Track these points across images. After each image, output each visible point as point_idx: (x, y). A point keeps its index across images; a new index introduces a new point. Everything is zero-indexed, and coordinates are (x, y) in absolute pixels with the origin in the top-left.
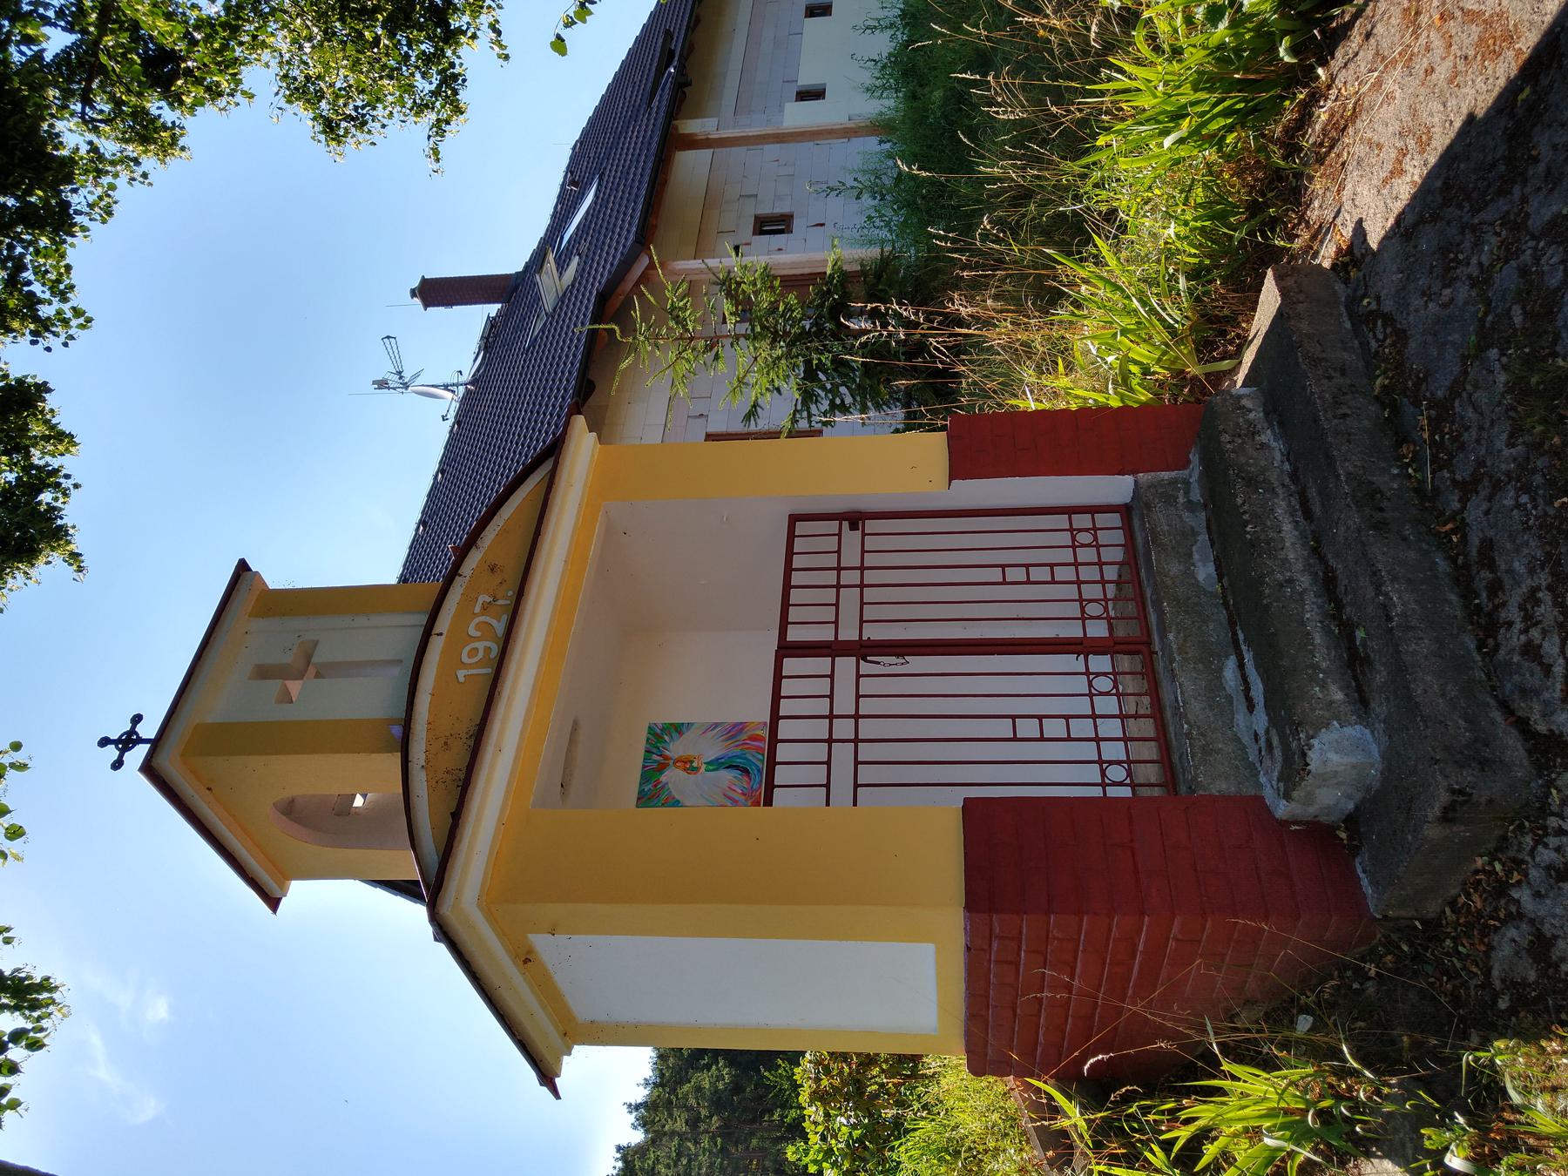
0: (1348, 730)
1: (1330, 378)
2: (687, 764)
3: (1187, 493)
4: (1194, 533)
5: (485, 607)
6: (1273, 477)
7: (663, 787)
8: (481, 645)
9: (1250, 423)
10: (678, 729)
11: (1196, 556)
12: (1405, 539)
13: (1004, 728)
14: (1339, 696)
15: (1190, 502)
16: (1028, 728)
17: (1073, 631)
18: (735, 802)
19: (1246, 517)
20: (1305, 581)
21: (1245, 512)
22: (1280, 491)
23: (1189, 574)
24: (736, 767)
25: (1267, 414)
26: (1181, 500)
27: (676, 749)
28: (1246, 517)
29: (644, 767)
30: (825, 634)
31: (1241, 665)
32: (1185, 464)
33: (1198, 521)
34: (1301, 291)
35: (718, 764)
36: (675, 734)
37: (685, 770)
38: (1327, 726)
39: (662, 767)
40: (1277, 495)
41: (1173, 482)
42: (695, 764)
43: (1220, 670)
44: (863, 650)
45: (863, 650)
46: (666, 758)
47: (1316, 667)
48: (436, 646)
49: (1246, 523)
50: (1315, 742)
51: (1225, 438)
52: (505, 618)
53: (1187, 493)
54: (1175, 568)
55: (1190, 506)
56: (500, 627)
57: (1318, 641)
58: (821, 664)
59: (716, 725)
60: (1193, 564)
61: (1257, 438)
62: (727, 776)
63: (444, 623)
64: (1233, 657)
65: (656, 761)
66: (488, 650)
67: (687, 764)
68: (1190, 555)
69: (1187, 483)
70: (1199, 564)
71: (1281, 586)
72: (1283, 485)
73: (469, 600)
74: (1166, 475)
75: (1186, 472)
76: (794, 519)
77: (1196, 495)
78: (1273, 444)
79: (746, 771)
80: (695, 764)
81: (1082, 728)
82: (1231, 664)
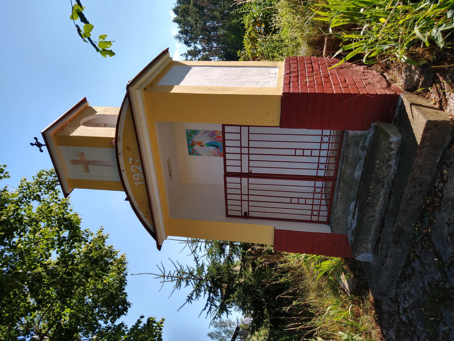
0: (368, 255)
1: (414, 187)
2: (200, 144)
3: (364, 142)
4: (360, 159)
5: (133, 163)
6: (386, 181)
7: (195, 151)
8: (137, 175)
9: (390, 156)
10: (195, 132)
11: (357, 168)
12: (401, 246)
13: (288, 200)
14: (370, 246)
15: (363, 146)
17: (313, 173)
18: (216, 156)
19: (370, 194)
20: (377, 216)
21: (370, 193)
22: (385, 186)
23: (353, 174)
24: (215, 146)
25: (398, 152)
26: (361, 144)
27: (196, 139)
28: (370, 194)
29: (188, 144)
30: (238, 170)
31: (356, 205)
32: (367, 128)
33: (363, 154)
34: (430, 140)
35: (209, 144)
36: (194, 135)
37: (200, 146)
38: (363, 253)
39: (193, 145)
40: (384, 187)
41: (361, 136)
42: (202, 144)
43: (350, 205)
44: (250, 175)
45: (250, 175)
46: (194, 142)
47: (368, 240)
48: (124, 174)
49: (369, 196)
50: (358, 256)
51: (378, 162)
52: (140, 166)
53: (364, 142)
54: (348, 171)
55: (363, 148)
56: (140, 169)
57: (372, 233)
58: (237, 180)
59: (206, 132)
60: (355, 171)
61: (389, 162)
62: (213, 148)
63: (123, 167)
64: (355, 202)
65: (191, 143)
66: (139, 176)
67: (200, 144)
68: (355, 167)
69: (366, 137)
70: (357, 171)
71: (370, 217)
72: (388, 184)
73: (126, 161)
74: (359, 132)
75: (367, 132)
76: (227, 216)
77: (367, 144)
78: (393, 166)
79: (217, 147)
80: (202, 144)
81: (316, 153)
82: (354, 203)
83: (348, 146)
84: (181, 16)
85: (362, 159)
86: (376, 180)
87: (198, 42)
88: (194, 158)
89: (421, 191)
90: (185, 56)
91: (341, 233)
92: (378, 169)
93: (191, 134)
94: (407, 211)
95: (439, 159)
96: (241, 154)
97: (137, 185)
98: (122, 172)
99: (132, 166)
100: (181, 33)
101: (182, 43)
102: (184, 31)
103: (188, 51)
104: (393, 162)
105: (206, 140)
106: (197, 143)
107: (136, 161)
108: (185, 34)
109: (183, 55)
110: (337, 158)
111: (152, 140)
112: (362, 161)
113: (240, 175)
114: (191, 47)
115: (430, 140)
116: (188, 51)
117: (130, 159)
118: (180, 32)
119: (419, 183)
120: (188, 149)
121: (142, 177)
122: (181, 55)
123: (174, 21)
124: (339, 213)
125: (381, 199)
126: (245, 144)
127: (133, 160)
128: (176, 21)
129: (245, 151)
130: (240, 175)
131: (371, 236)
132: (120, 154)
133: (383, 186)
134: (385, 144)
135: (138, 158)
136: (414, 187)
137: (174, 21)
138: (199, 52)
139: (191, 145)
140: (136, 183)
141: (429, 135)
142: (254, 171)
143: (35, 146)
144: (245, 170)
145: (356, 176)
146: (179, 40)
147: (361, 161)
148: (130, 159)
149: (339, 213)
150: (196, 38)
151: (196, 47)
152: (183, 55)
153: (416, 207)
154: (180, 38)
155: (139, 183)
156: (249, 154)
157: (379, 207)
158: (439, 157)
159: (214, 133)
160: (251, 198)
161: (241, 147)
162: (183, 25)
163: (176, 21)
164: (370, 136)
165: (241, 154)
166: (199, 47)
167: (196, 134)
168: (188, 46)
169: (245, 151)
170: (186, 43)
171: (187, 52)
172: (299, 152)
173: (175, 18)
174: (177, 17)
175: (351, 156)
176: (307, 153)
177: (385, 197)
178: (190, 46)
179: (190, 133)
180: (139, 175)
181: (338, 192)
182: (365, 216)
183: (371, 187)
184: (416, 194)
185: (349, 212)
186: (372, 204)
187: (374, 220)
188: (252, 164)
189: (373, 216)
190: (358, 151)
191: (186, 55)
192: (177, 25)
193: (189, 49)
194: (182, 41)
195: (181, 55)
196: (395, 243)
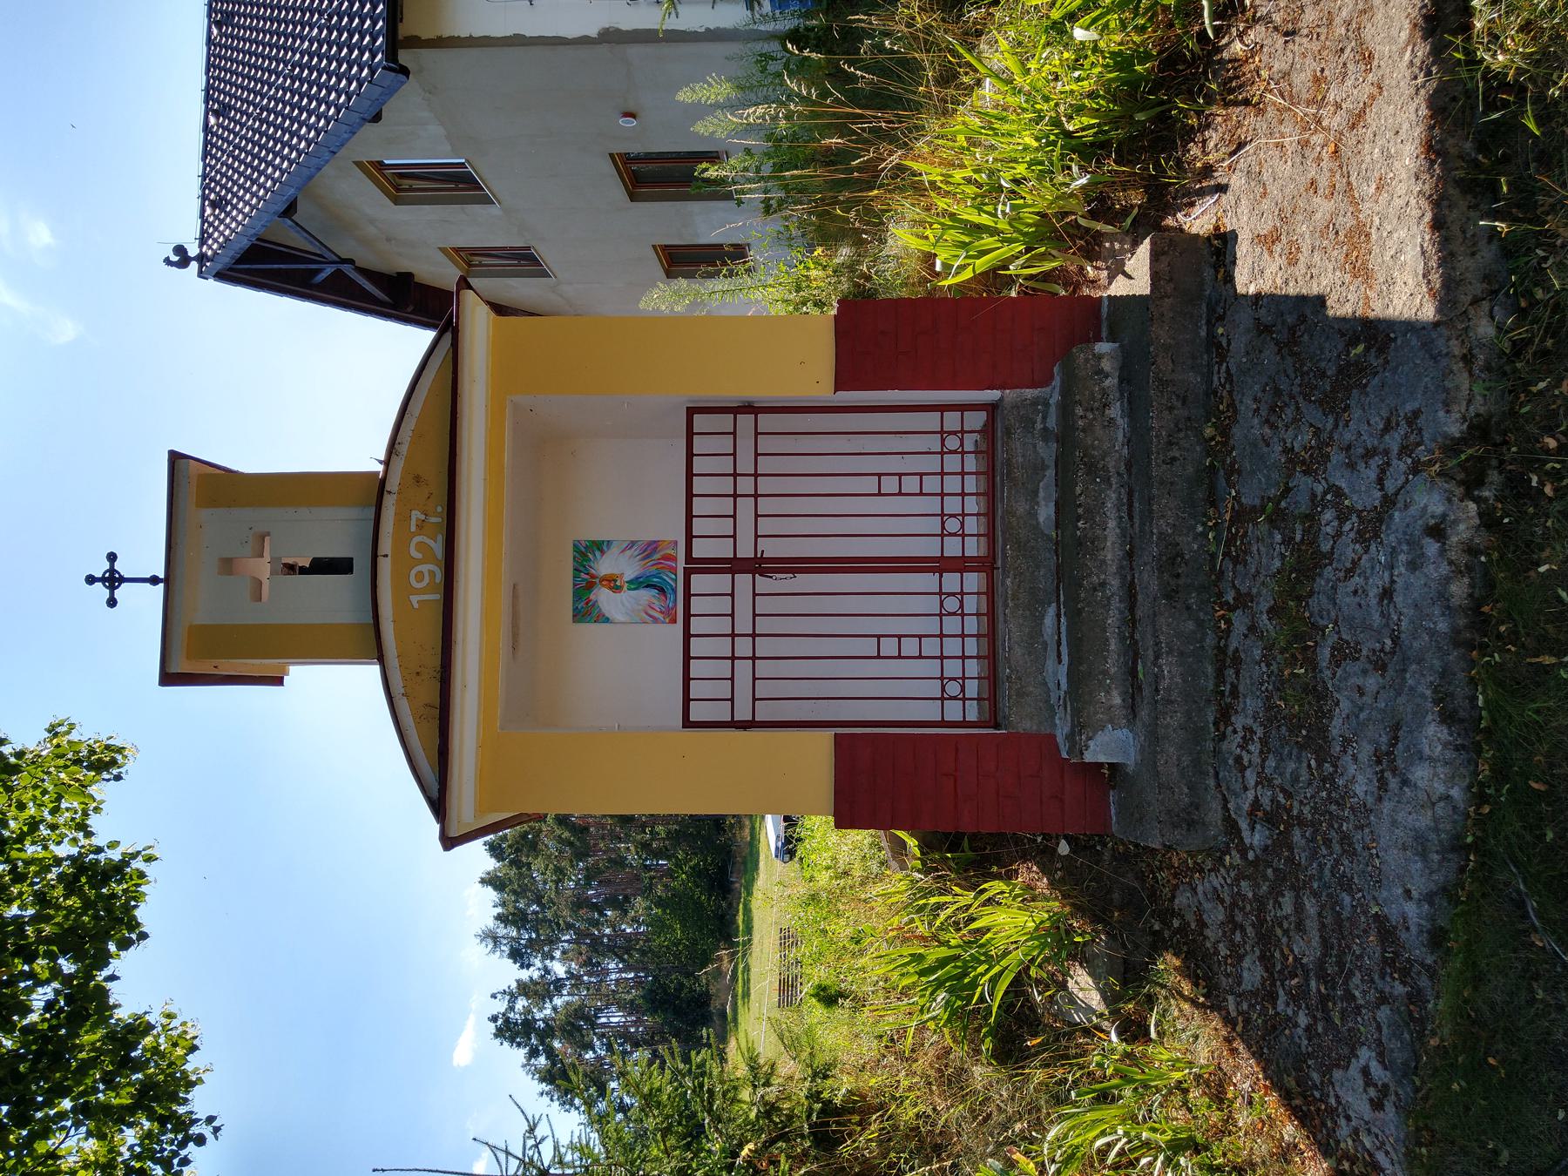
0: (1118, 733)
1: (1171, 409)
2: (612, 583)
3: (1044, 418)
4: (1044, 467)
5: (421, 526)
6: (1111, 463)
7: (593, 605)
8: (425, 568)
9: (1104, 392)
10: (599, 547)
11: (1041, 494)
12: (1188, 608)
13: (869, 647)
14: (1117, 701)
15: (1045, 429)
16: (889, 647)
17: (930, 548)
18: (655, 620)
19: (1080, 511)
20: (1115, 583)
21: (1080, 505)
22: (1114, 480)
23: (1033, 514)
24: (653, 586)
25: (1121, 381)
26: (1039, 426)
28: (1080, 511)
29: (575, 585)
30: (723, 550)
31: (1058, 616)
32: (1046, 381)
33: (1047, 452)
34: (1171, 280)
35: (639, 583)
36: (598, 554)
37: (611, 588)
38: (1103, 728)
39: (590, 586)
40: (1111, 485)
41: (1035, 402)
42: (618, 583)
43: (1042, 617)
44: (758, 566)
45: (758, 566)
46: (593, 577)
47: (1105, 673)
48: (385, 566)
49: (1079, 518)
50: (1091, 743)
51: (1079, 411)
52: (441, 539)
53: (1044, 418)
54: (1021, 508)
55: (1046, 434)
56: (438, 547)
57: (1113, 647)
58: (721, 582)
59: (633, 543)
60: (1037, 503)
61: (1107, 412)
62: (646, 595)
63: (386, 545)
64: (1054, 605)
65: (584, 580)
66: (432, 573)
67: (612, 583)
68: (1036, 493)
69: (1046, 404)
70: (1043, 503)
71: (1095, 589)
72: (1118, 473)
73: (402, 519)
74: (1029, 393)
75: (1048, 389)
77: (1052, 422)
78: (1120, 421)
79: (662, 590)
80: (618, 583)
82: (1052, 611)
83: (1008, 432)
84: (512, 863)
85: (1048, 467)
86: (1085, 464)
87: (557, 954)
88: (589, 629)
89: (1189, 419)
90: (508, 997)
91: (1035, 728)
92: (1084, 430)
93: (586, 552)
94: (1172, 483)
95: (1204, 328)
96: (735, 496)
97: (416, 606)
98: (381, 560)
99: (417, 539)
100: (502, 922)
101: (501, 957)
102: (513, 914)
103: (518, 981)
104: (1115, 411)
105: (627, 567)
106: (603, 579)
107: (433, 520)
108: (514, 923)
109: (499, 996)
110: (990, 473)
111: (493, 451)
112: (1050, 473)
113: (734, 566)
114: (532, 969)
115: (1171, 280)
116: (518, 981)
117: (416, 515)
118: (499, 918)
119: (1178, 396)
120: (574, 602)
121: (439, 577)
122: (494, 996)
123: (483, 881)
124: (1018, 651)
125: (1112, 524)
126: (745, 465)
127: (423, 517)
128: (491, 881)
129: (745, 485)
130: (734, 566)
131: (1113, 665)
132: (389, 492)
133: (1107, 480)
134: (1087, 360)
135: (439, 509)
136: (1171, 409)
137: (483, 881)
138: (558, 984)
139: (585, 585)
140: (415, 599)
141: (1163, 266)
142: (771, 549)
143: (107, 566)
144: (745, 551)
145: (1041, 520)
146: (491, 946)
147: (1047, 473)
148: (416, 515)
149: (1018, 651)
150: (552, 941)
151: (547, 971)
152: (499, 996)
153: (1190, 470)
154: (495, 940)
155: (426, 597)
156: (756, 496)
157: (1111, 551)
158: (1203, 322)
159: (651, 548)
160: (765, 485)
161: (735, 475)
162: (514, 892)
163: (491, 881)
164: (1056, 398)
165: (735, 496)
166: (559, 969)
167: (603, 552)
168: (522, 967)
169: (745, 485)
170: (517, 955)
171: (514, 985)
172: (890, 485)
173: (489, 873)
174: (495, 870)
175: (1020, 460)
176: (911, 484)
177: (1121, 518)
178: (528, 966)
179: (586, 547)
180: (431, 571)
181: (1005, 576)
182: (1081, 586)
183: (1078, 490)
184: (1180, 430)
185: (1045, 644)
186: (1093, 543)
187: (1109, 599)
188: (766, 526)
189: (1103, 584)
190: (1035, 446)
191: (512, 994)
192: (491, 894)
193: (525, 975)
194: (503, 948)
195: (494, 996)
196: (1168, 597)
